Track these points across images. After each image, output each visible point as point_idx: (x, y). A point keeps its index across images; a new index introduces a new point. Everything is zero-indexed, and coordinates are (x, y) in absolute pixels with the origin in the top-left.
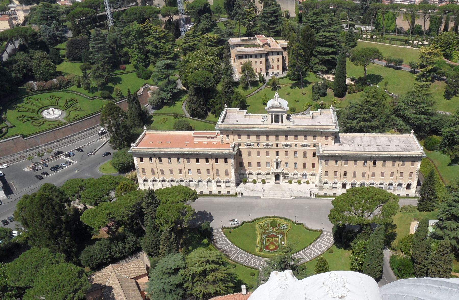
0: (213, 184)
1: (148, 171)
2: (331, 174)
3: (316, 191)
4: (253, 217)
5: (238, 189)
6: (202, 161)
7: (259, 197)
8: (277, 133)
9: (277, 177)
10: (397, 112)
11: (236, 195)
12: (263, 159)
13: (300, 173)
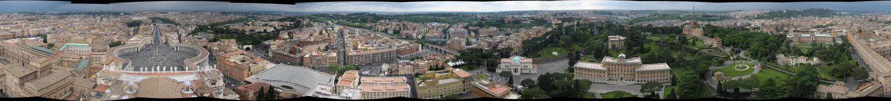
0: (599, 79)
1: (578, 73)
2: (640, 77)
3: (635, 83)
4: (612, 91)
5: (608, 82)
6: (596, 72)
7: (615, 85)
8: (622, 65)
9: (622, 79)
10: (660, 57)
11: (606, 84)
12: (617, 73)
13: (629, 77)
